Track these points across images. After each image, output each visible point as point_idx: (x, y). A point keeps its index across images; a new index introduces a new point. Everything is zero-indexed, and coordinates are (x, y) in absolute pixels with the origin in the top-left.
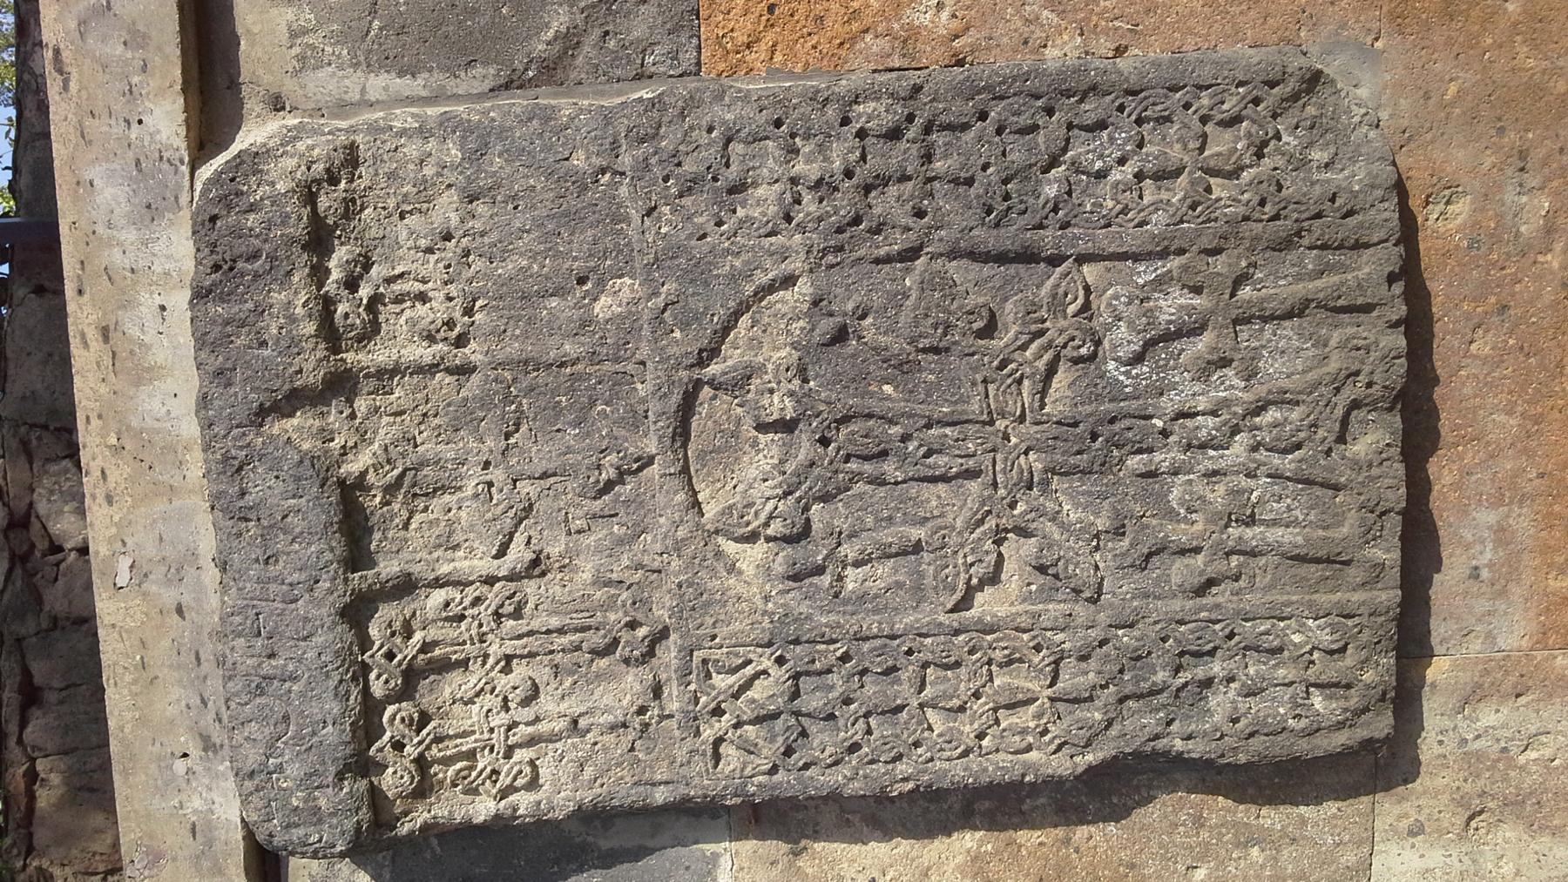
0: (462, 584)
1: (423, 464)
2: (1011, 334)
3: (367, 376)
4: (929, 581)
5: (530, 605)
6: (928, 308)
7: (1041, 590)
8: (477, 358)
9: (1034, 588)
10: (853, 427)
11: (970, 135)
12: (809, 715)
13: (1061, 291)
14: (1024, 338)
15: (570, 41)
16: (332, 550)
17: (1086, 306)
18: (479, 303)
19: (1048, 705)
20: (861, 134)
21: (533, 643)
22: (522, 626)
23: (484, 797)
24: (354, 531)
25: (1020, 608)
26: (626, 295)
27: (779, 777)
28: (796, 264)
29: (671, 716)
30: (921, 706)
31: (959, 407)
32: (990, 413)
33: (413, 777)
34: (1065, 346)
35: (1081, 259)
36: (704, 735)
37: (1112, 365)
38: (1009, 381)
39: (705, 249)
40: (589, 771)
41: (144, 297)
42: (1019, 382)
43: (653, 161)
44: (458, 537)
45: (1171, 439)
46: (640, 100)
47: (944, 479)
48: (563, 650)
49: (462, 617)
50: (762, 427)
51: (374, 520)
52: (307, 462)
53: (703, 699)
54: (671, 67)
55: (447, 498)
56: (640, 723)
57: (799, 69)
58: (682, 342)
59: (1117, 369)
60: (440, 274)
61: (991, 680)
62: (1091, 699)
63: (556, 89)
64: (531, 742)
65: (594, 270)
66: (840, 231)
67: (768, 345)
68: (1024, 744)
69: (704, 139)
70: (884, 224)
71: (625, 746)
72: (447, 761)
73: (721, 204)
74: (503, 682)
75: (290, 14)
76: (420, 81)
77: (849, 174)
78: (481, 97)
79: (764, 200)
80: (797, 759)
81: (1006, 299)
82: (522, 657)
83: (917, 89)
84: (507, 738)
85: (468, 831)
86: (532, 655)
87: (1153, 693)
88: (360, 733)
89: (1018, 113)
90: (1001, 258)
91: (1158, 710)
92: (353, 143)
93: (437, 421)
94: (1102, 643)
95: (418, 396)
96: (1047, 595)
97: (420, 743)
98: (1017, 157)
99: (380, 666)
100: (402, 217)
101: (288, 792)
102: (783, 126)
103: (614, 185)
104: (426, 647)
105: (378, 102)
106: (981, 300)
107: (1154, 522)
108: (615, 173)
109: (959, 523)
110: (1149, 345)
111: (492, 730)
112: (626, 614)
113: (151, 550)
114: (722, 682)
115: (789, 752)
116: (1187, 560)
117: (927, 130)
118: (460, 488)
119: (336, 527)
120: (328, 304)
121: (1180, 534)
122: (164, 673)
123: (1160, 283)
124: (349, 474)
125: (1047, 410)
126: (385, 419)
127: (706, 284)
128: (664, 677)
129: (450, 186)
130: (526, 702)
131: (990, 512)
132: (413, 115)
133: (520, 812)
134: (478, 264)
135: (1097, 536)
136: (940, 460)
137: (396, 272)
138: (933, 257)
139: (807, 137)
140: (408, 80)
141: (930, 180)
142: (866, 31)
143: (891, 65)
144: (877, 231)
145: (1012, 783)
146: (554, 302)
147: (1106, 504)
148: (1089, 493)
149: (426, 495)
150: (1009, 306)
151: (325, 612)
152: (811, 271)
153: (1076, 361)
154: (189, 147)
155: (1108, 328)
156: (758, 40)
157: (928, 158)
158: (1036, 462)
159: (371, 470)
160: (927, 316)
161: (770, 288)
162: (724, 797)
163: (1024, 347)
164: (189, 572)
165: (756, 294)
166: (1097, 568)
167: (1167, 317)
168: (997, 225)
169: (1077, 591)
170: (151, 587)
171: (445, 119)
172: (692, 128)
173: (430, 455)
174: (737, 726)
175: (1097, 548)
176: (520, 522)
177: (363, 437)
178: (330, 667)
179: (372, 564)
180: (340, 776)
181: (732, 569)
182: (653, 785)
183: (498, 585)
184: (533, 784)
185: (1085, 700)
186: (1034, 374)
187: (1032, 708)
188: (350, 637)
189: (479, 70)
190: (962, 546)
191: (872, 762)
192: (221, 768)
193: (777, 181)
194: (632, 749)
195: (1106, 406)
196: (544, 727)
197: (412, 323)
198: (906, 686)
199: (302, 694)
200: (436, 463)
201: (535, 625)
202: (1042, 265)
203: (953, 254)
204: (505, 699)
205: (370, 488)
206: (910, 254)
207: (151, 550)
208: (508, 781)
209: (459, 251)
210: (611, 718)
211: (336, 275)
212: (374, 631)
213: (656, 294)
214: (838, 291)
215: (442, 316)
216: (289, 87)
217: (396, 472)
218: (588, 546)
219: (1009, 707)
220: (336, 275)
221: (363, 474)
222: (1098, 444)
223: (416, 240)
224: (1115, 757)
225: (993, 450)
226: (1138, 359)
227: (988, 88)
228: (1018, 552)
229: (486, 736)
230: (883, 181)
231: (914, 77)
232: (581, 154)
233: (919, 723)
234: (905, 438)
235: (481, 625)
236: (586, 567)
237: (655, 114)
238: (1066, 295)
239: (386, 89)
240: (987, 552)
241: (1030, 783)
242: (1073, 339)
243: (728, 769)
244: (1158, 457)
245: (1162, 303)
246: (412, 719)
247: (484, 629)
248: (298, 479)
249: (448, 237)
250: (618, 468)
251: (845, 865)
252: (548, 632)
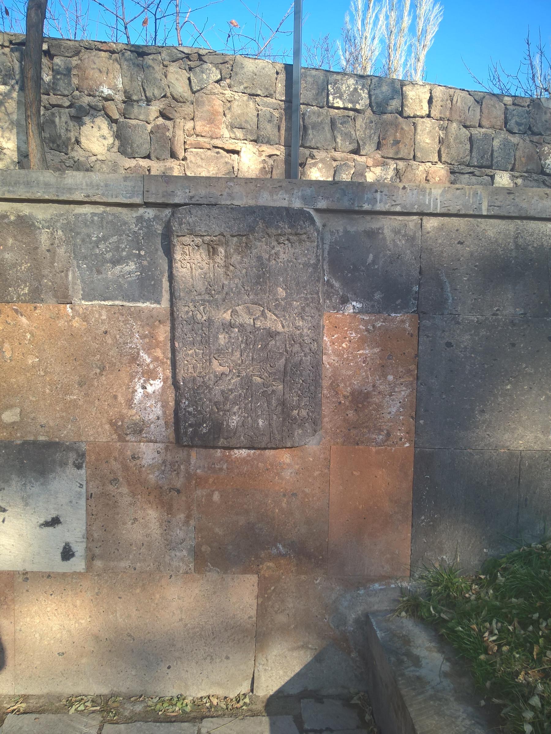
41: (287, 195)
75: (341, 230)
96: (216, 376)
101: (186, 218)
113: (235, 190)
122: (208, 190)
140: (327, 253)
170: (227, 190)
181: (225, 312)
199: (206, 224)
207: (235, 190)
216: (327, 229)
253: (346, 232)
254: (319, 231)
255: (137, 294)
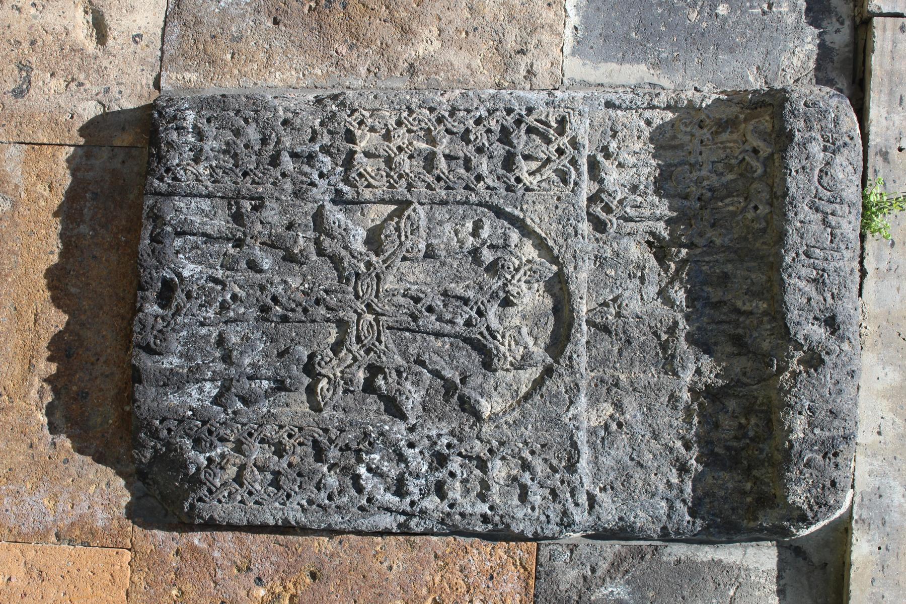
46: (574, 532)
76: (709, 557)
154: (852, 529)
164: (884, 266)
192: (878, 140)
239: (730, 554)
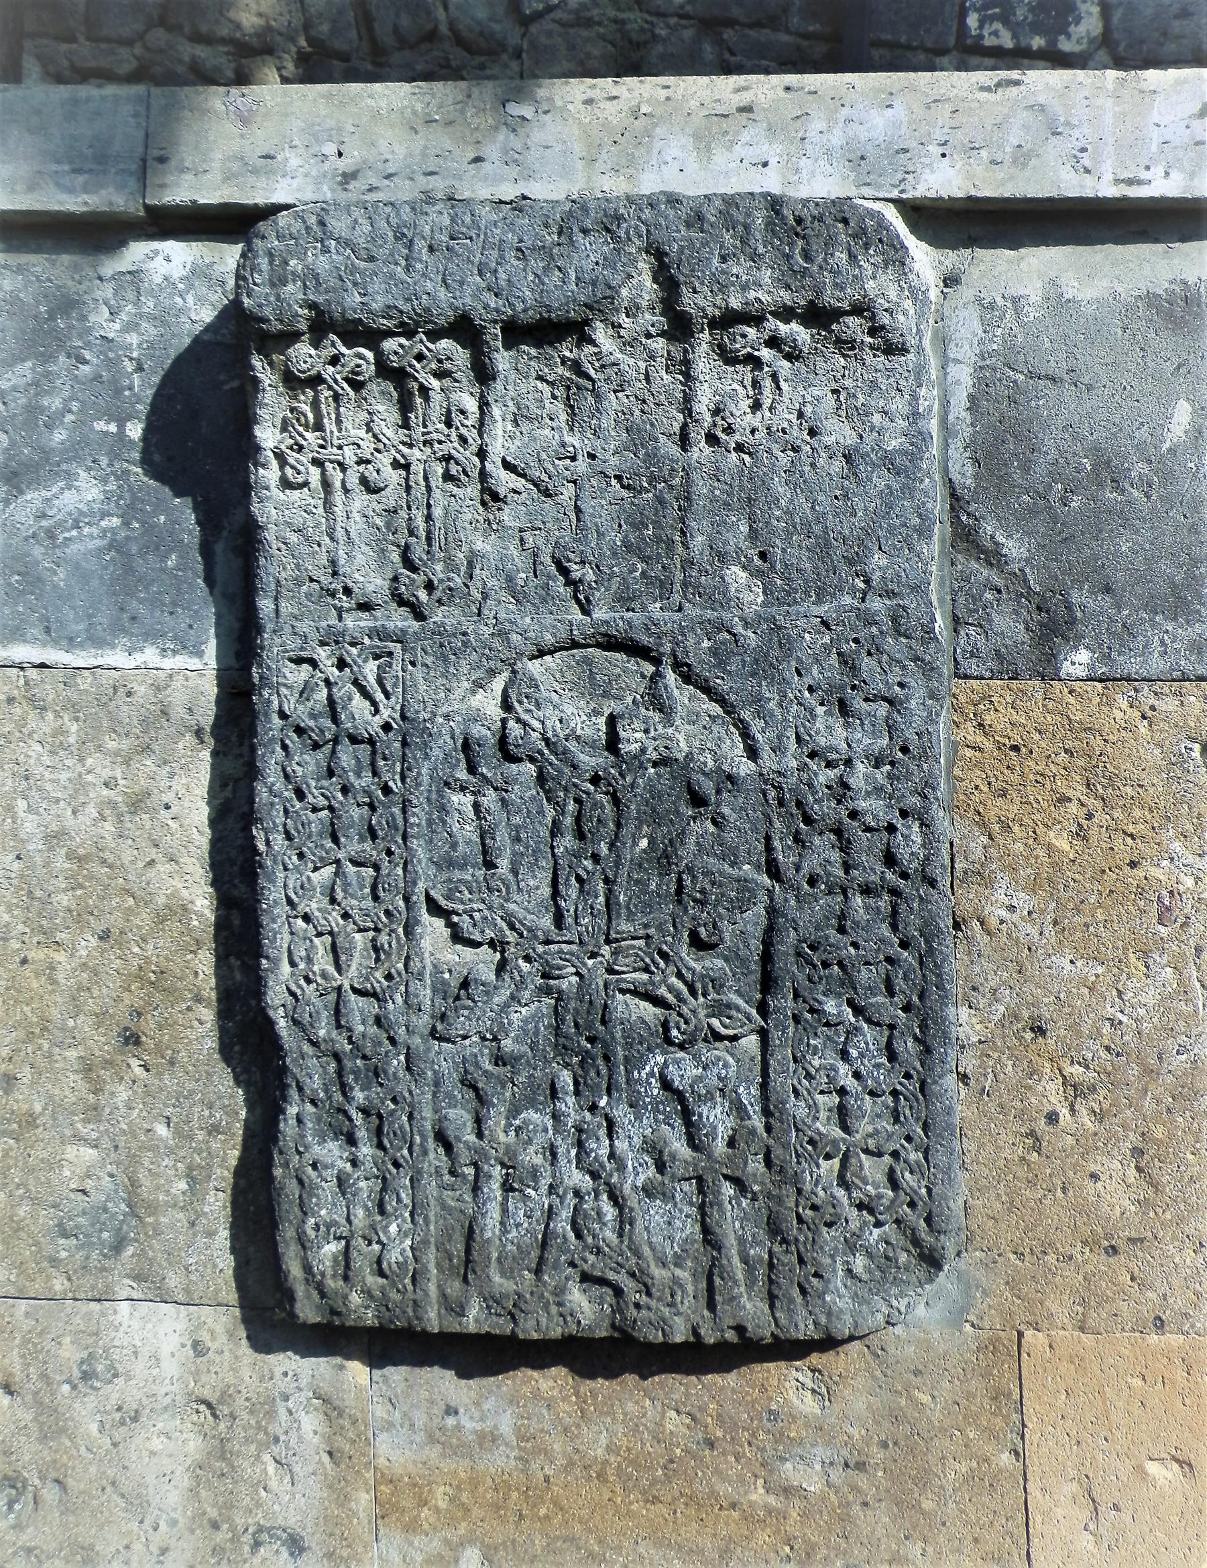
0: (481, 427)
1: (598, 397)
2: (692, 964)
3: (686, 351)
4: (457, 874)
5: (455, 490)
6: (720, 886)
7: (444, 983)
8: (695, 454)
9: (447, 976)
10: (608, 808)
11: (885, 930)
12: (334, 752)
13: (733, 1013)
14: (689, 976)
15: (993, 557)
16: (525, 311)
17: (718, 1037)
18: (747, 458)
19: (334, 984)
20: (891, 829)
21: (419, 491)
22: (437, 481)
23: (279, 437)
24: (540, 331)
25: (428, 962)
26: (747, 597)
27: (276, 721)
28: (768, 760)
29: (340, 618)
30: (337, 862)
31: (623, 911)
32: (617, 940)
33: (303, 372)
34: (680, 1015)
35: (763, 1034)
36: (320, 650)
37: (660, 1059)
38: (648, 960)
39: (787, 675)
40: (294, 538)
42: (646, 970)
43: (874, 629)
44: (525, 427)
45: (588, 1115)
46: (933, 620)
47: (555, 894)
48: (410, 519)
49: (449, 424)
50: (612, 720)
51: (550, 351)
52: (609, 293)
53: (354, 651)
54: (964, 651)
55: (563, 417)
56: (336, 589)
57: (957, 772)
58: (699, 648)
59: (656, 1064)
60: (777, 423)
61: (360, 931)
62: (339, 1026)
63: (949, 542)
64: (326, 484)
65: (773, 567)
66: (799, 804)
67: (692, 730)
68: (297, 960)
69: (894, 678)
70: (804, 847)
71: (315, 574)
72: (315, 405)
73: (829, 692)
74: (384, 461)
77: (853, 815)
78: (945, 470)
79: (831, 732)
80: (293, 739)
81: (726, 960)
82: (407, 479)
83: (932, 883)
84: (332, 462)
85: (245, 421)
86: (408, 489)
87: (344, 1088)
88: (351, 327)
89: (906, 978)
90: (767, 957)
91: (326, 1091)
92: (907, 351)
93: (637, 413)
94: (392, 1041)
95: (662, 398)
96: (440, 989)
97: (336, 381)
98: (864, 975)
99: (411, 347)
100: (834, 391)
101: (302, 257)
102: (901, 755)
103: (853, 591)
104: (424, 391)
105: (946, 374)
106: (727, 936)
107: (508, 1094)
108: (865, 593)
109: (512, 906)
110: (679, 1096)
111: (340, 448)
112: (441, 581)
114: (370, 669)
115: (300, 731)
116: (470, 1125)
117: (894, 892)
118: (572, 430)
119: (546, 315)
120: (756, 320)
121: (496, 1119)
123: (739, 1109)
124: (595, 330)
125: (619, 996)
126: (642, 365)
127: (753, 674)
128: (378, 614)
129: (861, 437)
130: (364, 481)
131: (521, 935)
132: (930, 407)
133: (261, 471)
134: (784, 460)
135: (495, 1039)
136: (573, 891)
137: (783, 384)
138: (770, 893)
139: (890, 776)
141: (844, 892)
142: (991, 838)
143: (957, 860)
144: (797, 839)
145: (259, 945)
146: (744, 528)
147: (525, 1049)
148: (536, 1033)
149: (568, 398)
150: (720, 963)
151: (467, 301)
152: (761, 775)
153: (665, 1025)
155: (696, 1057)
156: (986, 734)
157: (866, 890)
158: (569, 983)
159: (596, 350)
160: (713, 883)
161: (746, 735)
162: (260, 666)
163: (679, 975)
165: (741, 721)
166: (465, 1037)
167: (705, 1114)
168: (799, 954)
169: (443, 1017)
171: (925, 437)
172: (904, 668)
173: (606, 403)
174: (328, 682)
175: (484, 1039)
176: (535, 485)
177: (628, 344)
178: (416, 302)
179: (508, 346)
180: (313, 306)
182: (276, 599)
183: (476, 460)
184: (286, 484)
185: (338, 1021)
186: (653, 983)
187: (331, 969)
188: (442, 322)
189: (970, 470)
190: (490, 908)
191: (286, 811)
193: (849, 746)
194: (312, 580)
195: (620, 1053)
196: (338, 497)
197: (733, 395)
198: (358, 847)
199: (392, 275)
200: (598, 410)
201: (437, 494)
202: (759, 996)
203: (772, 911)
204: (368, 462)
205: (579, 346)
206: (773, 870)
208: (291, 461)
209: (799, 442)
210: (342, 562)
211: (784, 329)
212: (445, 344)
213: (746, 625)
214: (741, 800)
215: (736, 422)
217: (592, 372)
218: (507, 549)
219: (334, 947)
220: (784, 329)
221: (593, 342)
222: (584, 1043)
223: (811, 403)
224: (281, 1048)
225: (581, 942)
226: (666, 1085)
227: (931, 951)
228: (482, 962)
229: (336, 442)
230: (845, 844)
231: (944, 882)
232: (884, 562)
233: (321, 859)
234: (596, 858)
235: (440, 442)
236: (490, 546)
237: (919, 634)
238: (729, 1017)
239: (958, 382)
240: (483, 932)
241: (259, 965)
242: (686, 1023)
243: (286, 671)
244: (571, 1100)
245: (719, 1109)
246: (358, 374)
247: (436, 445)
248: (594, 283)
249: (812, 433)
250: (581, 581)
251: (184, 781)
252: (429, 506)
253: (1058, 304)
254: (926, 302)
255: (103, 619)
